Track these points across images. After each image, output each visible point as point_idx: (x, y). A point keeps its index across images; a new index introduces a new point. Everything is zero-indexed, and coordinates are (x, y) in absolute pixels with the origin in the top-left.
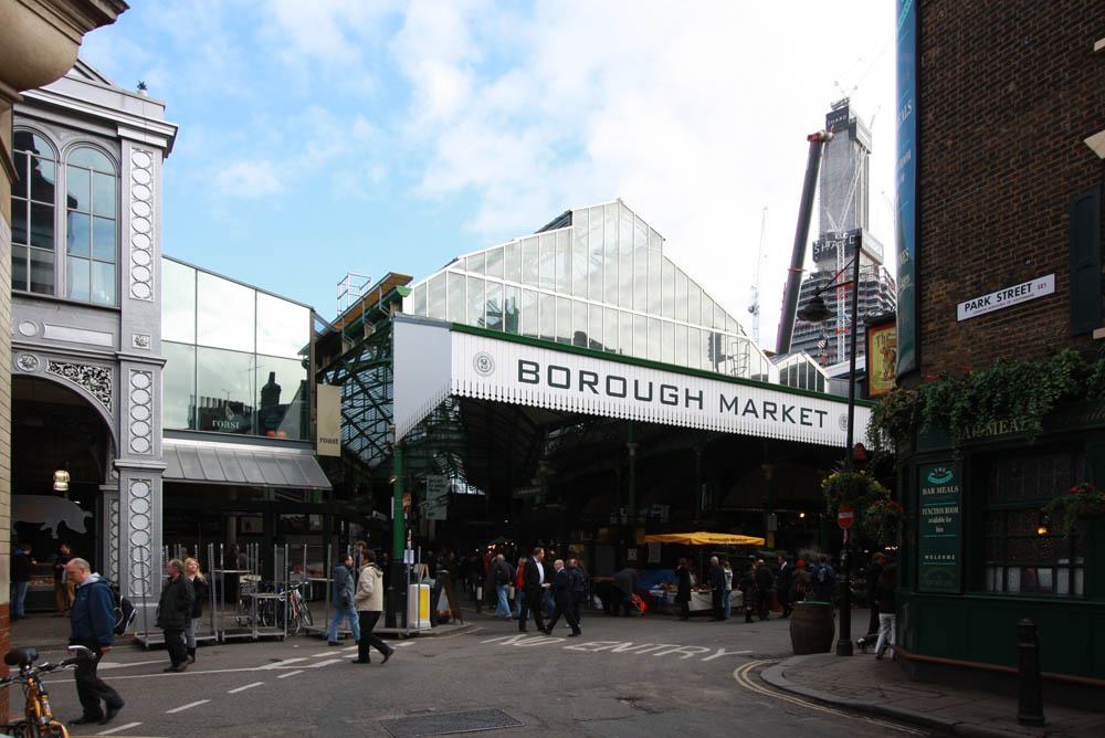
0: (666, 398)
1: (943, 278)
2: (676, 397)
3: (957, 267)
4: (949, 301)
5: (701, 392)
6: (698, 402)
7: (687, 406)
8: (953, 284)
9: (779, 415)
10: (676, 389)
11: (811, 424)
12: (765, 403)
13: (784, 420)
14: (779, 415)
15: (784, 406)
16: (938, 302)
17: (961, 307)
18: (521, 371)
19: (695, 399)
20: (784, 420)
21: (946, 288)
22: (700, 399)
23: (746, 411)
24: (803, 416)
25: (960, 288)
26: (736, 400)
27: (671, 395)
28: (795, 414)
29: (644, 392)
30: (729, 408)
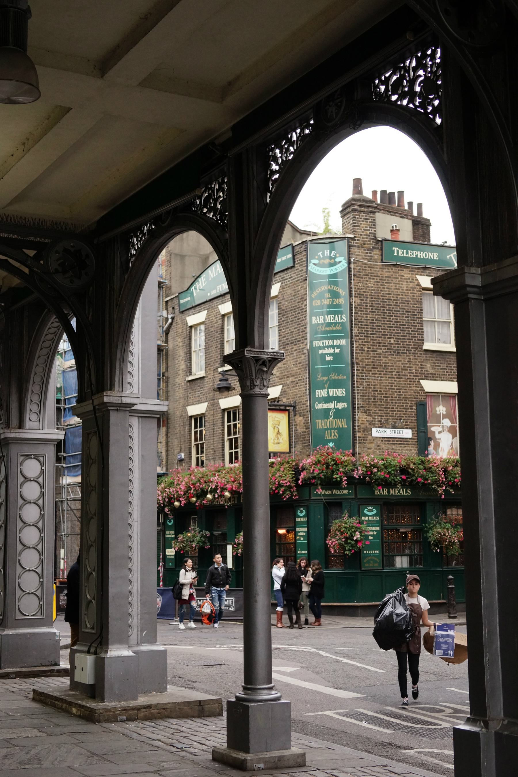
1: (365, 413)
3: (371, 410)
4: (367, 425)
8: (369, 417)
17: (374, 430)
21: (366, 418)
25: (372, 421)
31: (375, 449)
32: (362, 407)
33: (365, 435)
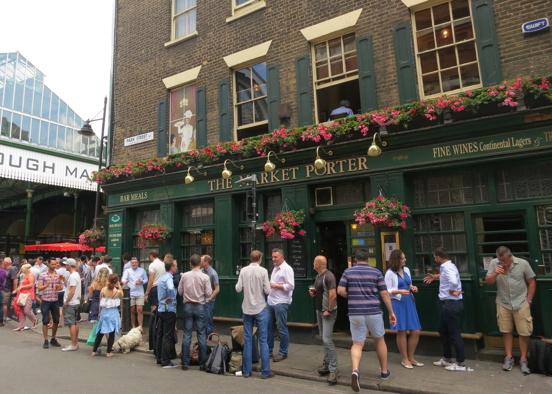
0: (31, 166)
2: (37, 166)
4: (122, 137)
5: (54, 164)
6: (52, 169)
7: (44, 171)
16: (118, 137)
17: (126, 140)
19: (50, 167)
22: (53, 168)
23: (82, 176)
26: (76, 169)
27: (34, 165)
29: (15, 162)
30: (71, 174)
31: (127, 158)
32: (119, 121)
33: (120, 146)
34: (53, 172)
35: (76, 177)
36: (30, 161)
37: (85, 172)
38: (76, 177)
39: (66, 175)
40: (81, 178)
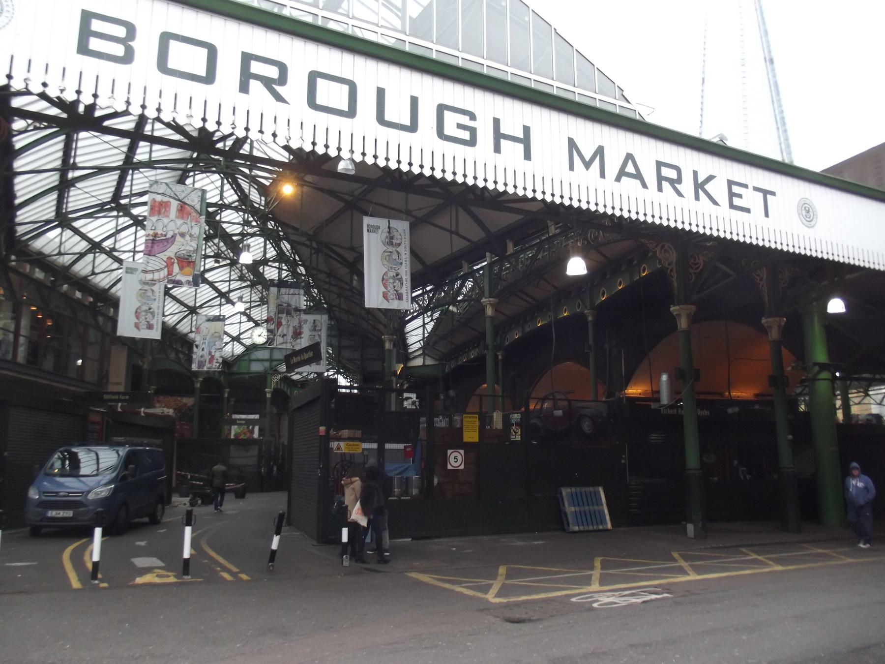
0: (450, 129)
2: (473, 131)
5: (527, 130)
6: (520, 147)
9: (687, 186)
10: (473, 117)
11: (748, 210)
12: (659, 165)
13: (697, 198)
14: (687, 186)
15: (695, 173)
18: (86, 32)
20: (697, 198)
22: (526, 140)
23: (622, 173)
24: (732, 195)
26: (600, 151)
27: (460, 126)
28: (718, 189)
29: (398, 112)
30: (587, 165)
34: (527, 156)
35: (603, 175)
36: (447, 114)
37: (630, 163)
38: (603, 175)
39: (572, 168)
40: (618, 179)
